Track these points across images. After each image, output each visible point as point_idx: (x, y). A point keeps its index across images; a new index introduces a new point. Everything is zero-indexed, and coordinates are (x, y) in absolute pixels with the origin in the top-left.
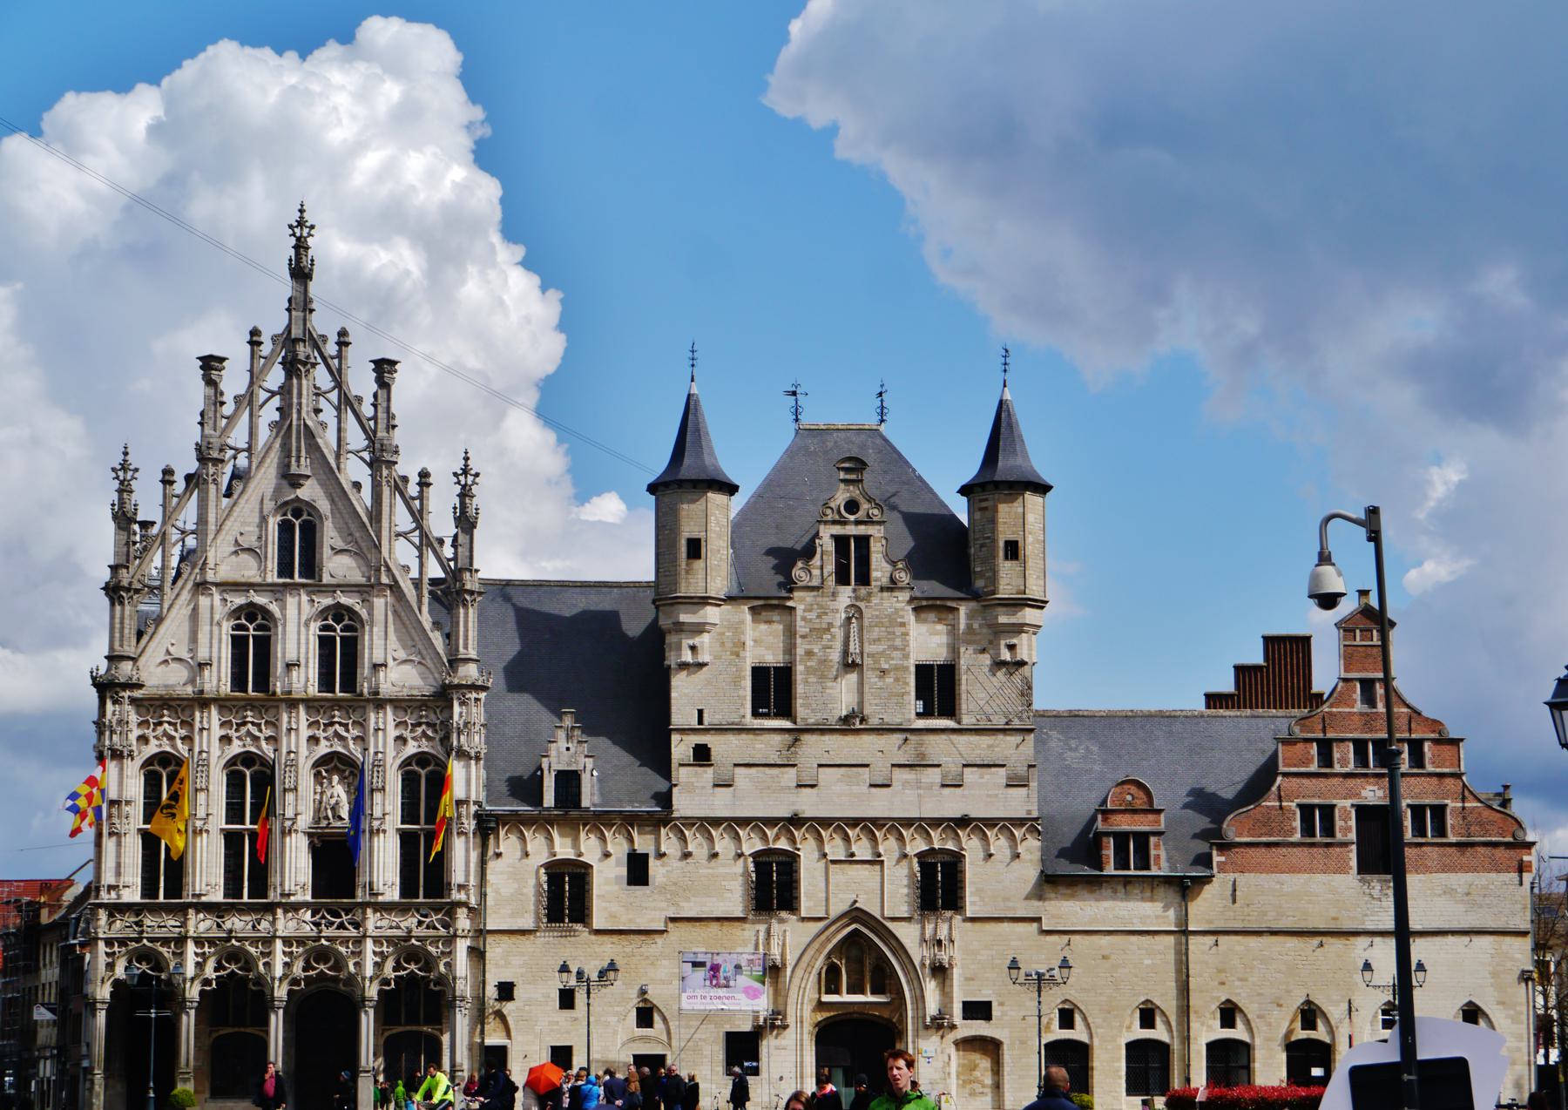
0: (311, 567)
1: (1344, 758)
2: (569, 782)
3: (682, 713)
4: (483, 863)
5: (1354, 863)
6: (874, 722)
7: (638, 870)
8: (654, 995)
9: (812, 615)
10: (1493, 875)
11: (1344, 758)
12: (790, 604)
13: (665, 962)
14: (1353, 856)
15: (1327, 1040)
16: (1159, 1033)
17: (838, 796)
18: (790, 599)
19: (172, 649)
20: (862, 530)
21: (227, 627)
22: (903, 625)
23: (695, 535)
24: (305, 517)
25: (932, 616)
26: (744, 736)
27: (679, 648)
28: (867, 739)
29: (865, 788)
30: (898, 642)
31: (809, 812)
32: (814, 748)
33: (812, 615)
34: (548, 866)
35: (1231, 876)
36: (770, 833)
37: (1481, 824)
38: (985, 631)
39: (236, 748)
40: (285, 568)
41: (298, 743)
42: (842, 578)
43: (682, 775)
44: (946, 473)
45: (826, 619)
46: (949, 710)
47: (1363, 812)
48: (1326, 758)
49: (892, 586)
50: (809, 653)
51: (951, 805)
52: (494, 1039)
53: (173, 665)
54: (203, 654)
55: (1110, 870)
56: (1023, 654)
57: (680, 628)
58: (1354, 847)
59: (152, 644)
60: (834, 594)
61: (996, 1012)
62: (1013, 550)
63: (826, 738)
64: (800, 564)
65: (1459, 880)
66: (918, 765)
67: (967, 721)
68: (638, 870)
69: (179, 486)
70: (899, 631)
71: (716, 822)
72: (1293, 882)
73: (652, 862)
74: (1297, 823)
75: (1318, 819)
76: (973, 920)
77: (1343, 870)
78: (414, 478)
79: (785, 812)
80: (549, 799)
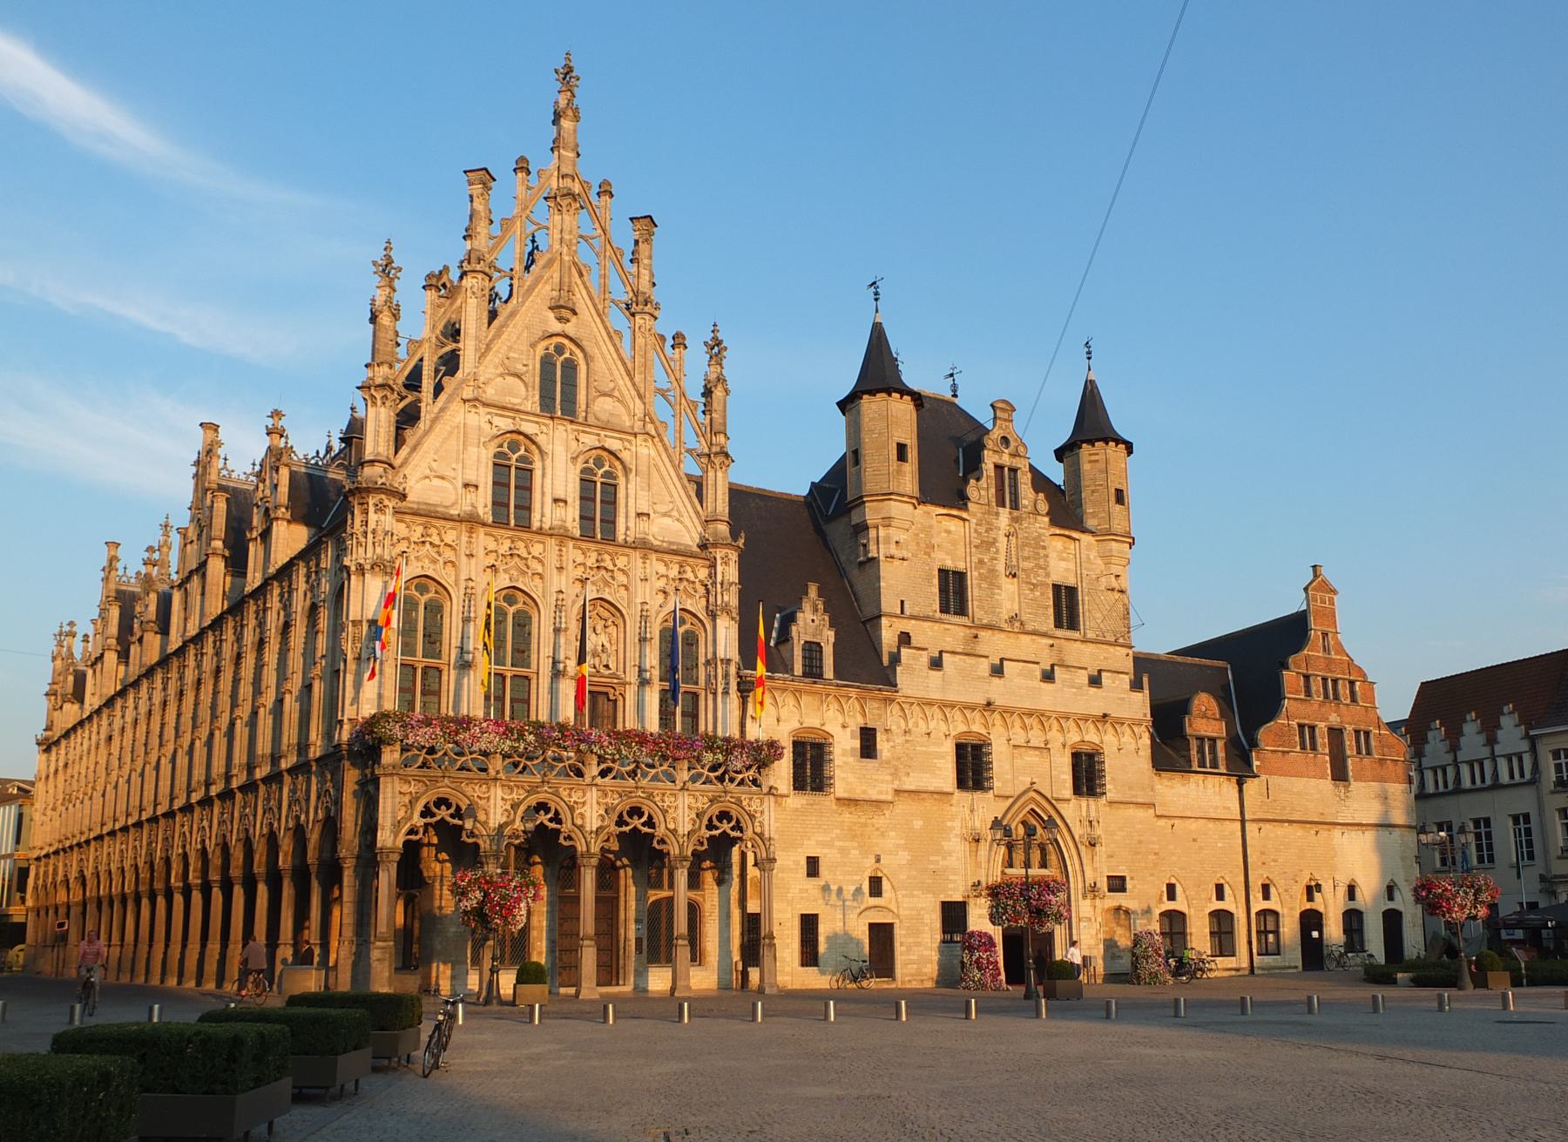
0: (570, 411)
1: (1316, 685)
2: (813, 650)
3: (889, 603)
6: (1029, 627)
7: (868, 744)
8: (886, 869)
9: (982, 530)
12: (965, 515)
13: (892, 834)
15: (1321, 909)
16: (1227, 904)
17: (1020, 687)
18: (964, 508)
19: (434, 465)
21: (487, 455)
22: (1044, 548)
23: (902, 441)
24: (567, 355)
25: (1058, 544)
27: (888, 540)
28: (1026, 639)
29: (1037, 683)
30: (1042, 562)
31: (999, 701)
34: (795, 732)
38: (1099, 561)
39: (504, 581)
42: (1001, 503)
44: (1040, 436)
45: (993, 534)
46: (1073, 624)
47: (1330, 729)
48: (1308, 693)
49: (1036, 512)
50: (981, 562)
51: (1095, 702)
52: (753, 907)
53: (436, 482)
54: (471, 477)
55: (1195, 767)
56: (1124, 583)
57: (888, 521)
59: (416, 458)
60: (997, 514)
61: (1129, 885)
62: (1120, 497)
67: (1090, 635)
68: (868, 744)
71: (930, 704)
72: (1299, 783)
73: (879, 737)
75: (1307, 733)
78: (670, 342)
80: (798, 669)
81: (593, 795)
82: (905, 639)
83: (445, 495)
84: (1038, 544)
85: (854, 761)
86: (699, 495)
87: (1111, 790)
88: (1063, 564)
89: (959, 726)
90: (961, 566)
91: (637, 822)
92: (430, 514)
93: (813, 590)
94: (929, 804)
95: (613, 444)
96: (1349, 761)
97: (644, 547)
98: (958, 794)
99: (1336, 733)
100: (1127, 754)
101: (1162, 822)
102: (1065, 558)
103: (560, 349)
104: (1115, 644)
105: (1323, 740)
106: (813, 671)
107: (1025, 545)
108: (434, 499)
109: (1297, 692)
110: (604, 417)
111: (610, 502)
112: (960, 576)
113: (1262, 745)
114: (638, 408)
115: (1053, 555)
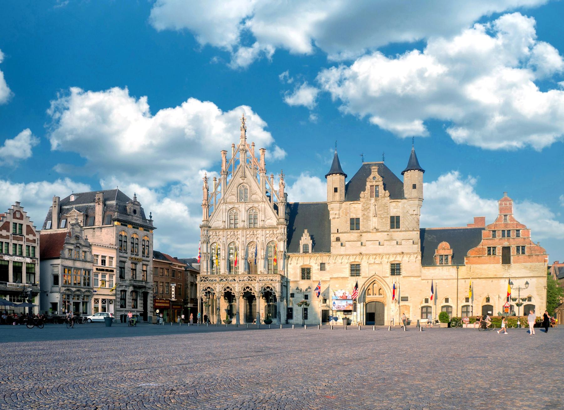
1: (499, 234)
3: (333, 230)
4: (287, 266)
5: (501, 261)
6: (380, 230)
7: (322, 267)
10: (537, 263)
11: (499, 234)
14: (501, 259)
17: (371, 247)
18: (359, 200)
20: (377, 184)
25: (394, 204)
26: (348, 234)
29: (378, 246)
30: (386, 211)
31: (363, 252)
32: (366, 236)
33: (365, 205)
35: (469, 265)
36: (355, 257)
37: (535, 251)
38: (408, 207)
40: (241, 198)
41: (241, 239)
43: (333, 244)
45: (368, 206)
47: (504, 248)
48: (494, 236)
49: (385, 197)
50: (364, 214)
51: (399, 249)
55: (438, 264)
57: (332, 209)
58: (501, 257)
60: (370, 200)
61: (409, 299)
63: (369, 234)
64: (362, 192)
65: (529, 264)
66: (392, 239)
68: (322, 267)
69: (218, 181)
70: (386, 208)
72: (485, 266)
73: (326, 265)
74: (487, 252)
76: (404, 277)
77: (498, 263)
79: (358, 252)
80: (301, 251)
81: (237, 285)
82: (338, 239)
83: (221, 225)
84: (385, 206)
85: (319, 271)
86: (277, 213)
87: (403, 272)
88: (396, 210)
89: (352, 260)
90: (358, 217)
91: (248, 290)
92: (216, 229)
93: (306, 231)
94: (341, 281)
95: (256, 205)
96: (512, 258)
97: (263, 228)
98: (350, 278)
99: (506, 250)
100: (411, 261)
101: (424, 281)
102: (396, 208)
103: (243, 186)
104: (413, 230)
105: (499, 252)
106: (306, 252)
107: (380, 207)
108: (217, 226)
109: (489, 236)
110: (254, 199)
111: (255, 218)
112: (358, 219)
113: (468, 255)
114: (261, 195)
115: (392, 208)
